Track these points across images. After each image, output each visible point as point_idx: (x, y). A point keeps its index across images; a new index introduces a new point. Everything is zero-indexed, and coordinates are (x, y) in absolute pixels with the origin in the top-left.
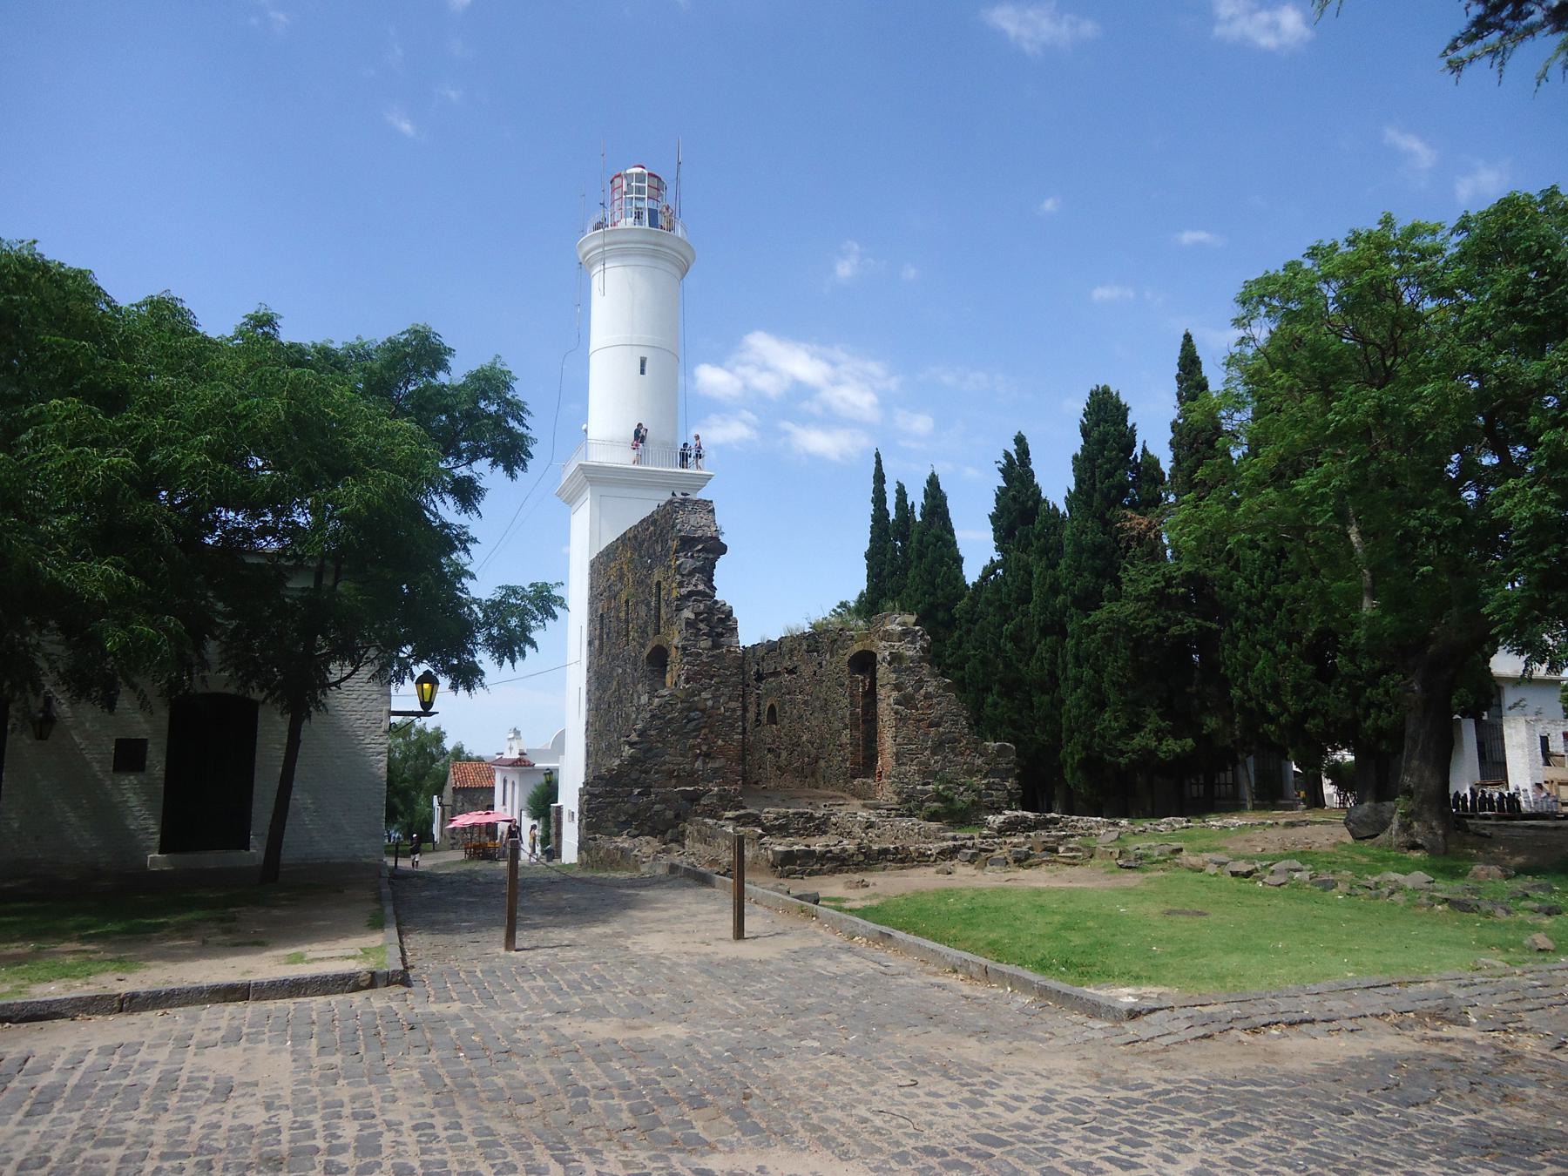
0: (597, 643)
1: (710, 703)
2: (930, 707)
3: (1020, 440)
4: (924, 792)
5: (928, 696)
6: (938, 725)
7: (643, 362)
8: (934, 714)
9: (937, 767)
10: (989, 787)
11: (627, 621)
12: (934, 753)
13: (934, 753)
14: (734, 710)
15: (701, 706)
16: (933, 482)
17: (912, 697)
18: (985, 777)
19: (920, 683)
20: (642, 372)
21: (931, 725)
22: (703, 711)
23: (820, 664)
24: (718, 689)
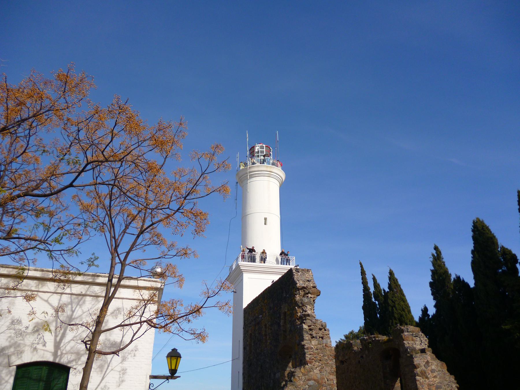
0: (248, 348)
1: (319, 376)
2: (435, 377)
3: (436, 248)
5: (433, 371)
7: (266, 219)
8: (437, 380)
11: (266, 335)
15: (315, 378)
16: (391, 273)
20: (265, 224)
22: (316, 381)
23: (362, 357)
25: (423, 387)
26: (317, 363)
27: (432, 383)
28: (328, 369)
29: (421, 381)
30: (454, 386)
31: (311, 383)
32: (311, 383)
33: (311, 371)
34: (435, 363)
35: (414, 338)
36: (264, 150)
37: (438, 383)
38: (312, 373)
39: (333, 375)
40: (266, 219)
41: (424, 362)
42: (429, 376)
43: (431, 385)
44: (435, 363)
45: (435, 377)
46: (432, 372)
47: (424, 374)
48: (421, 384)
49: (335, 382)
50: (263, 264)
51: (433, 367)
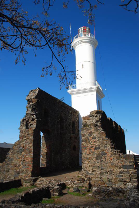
2: (95, 142)
4: (92, 174)
5: (94, 138)
6: (98, 148)
7: (83, 65)
9: (98, 164)
10: (121, 172)
12: (97, 159)
13: (97, 159)
14: (31, 147)
15: (22, 146)
17: (88, 139)
18: (120, 168)
19: (91, 133)
21: (96, 149)
22: (23, 147)
24: (27, 141)
25: (85, 148)
26: (24, 138)
27: (92, 146)
28: (29, 141)
29: (85, 145)
30: (109, 147)
31: (21, 148)
32: (21, 148)
33: (21, 143)
34: (96, 133)
35: (89, 118)
36: (83, 30)
37: (97, 145)
38: (21, 144)
39: (32, 144)
40: (83, 65)
41: (88, 132)
42: (90, 142)
43: (91, 147)
44: (96, 133)
45: (95, 142)
46: (93, 139)
47: (87, 141)
48: (84, 147)
49: (32, 147)
50: (75, 89)
51: (95, 135)
